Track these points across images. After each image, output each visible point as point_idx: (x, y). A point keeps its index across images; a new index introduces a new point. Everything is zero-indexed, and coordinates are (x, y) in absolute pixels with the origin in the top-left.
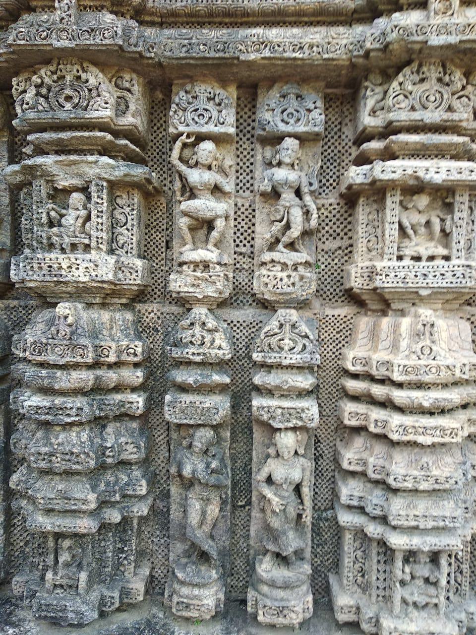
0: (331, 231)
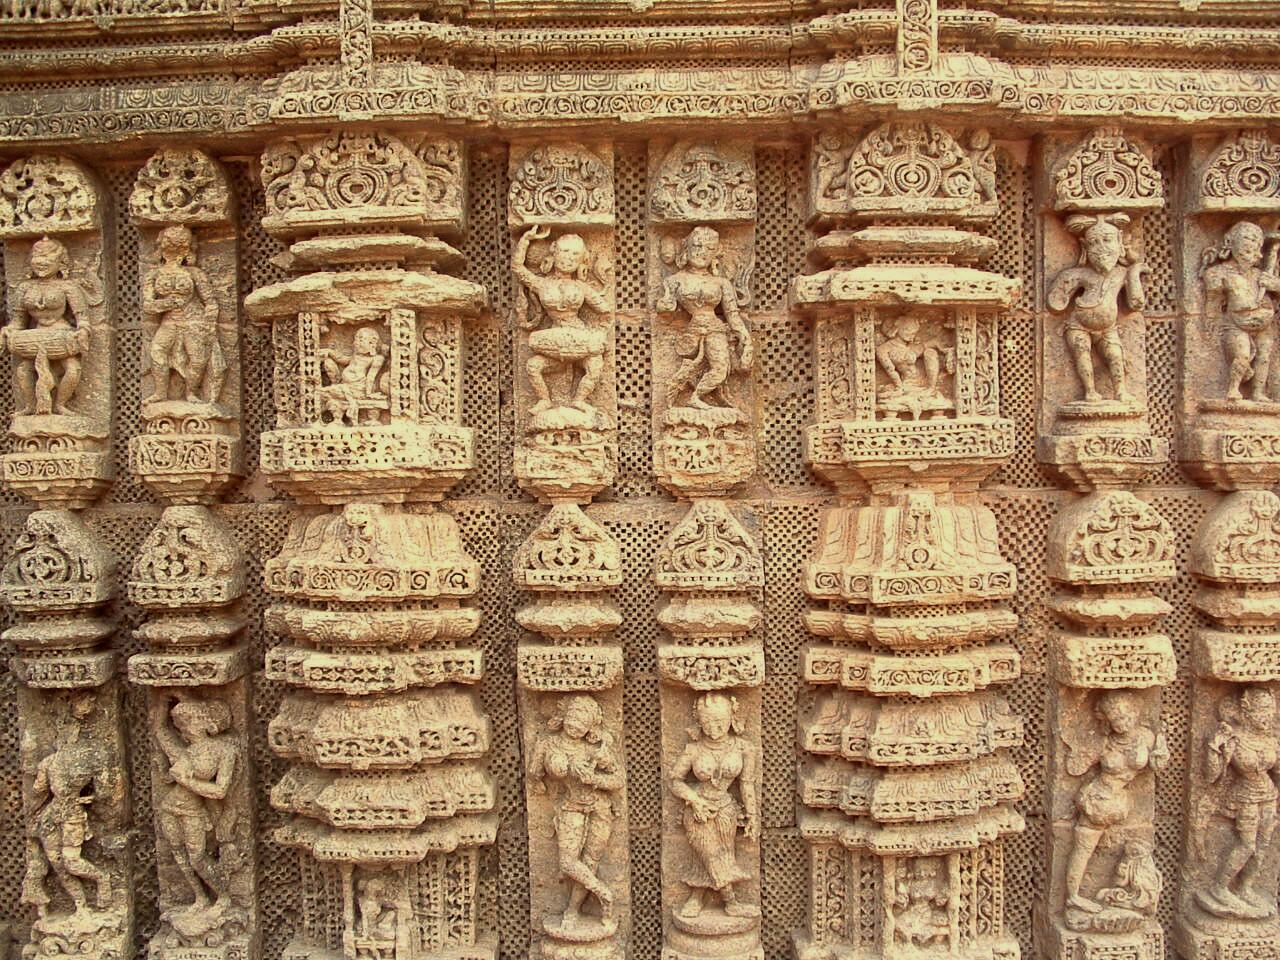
0: (778, 369)
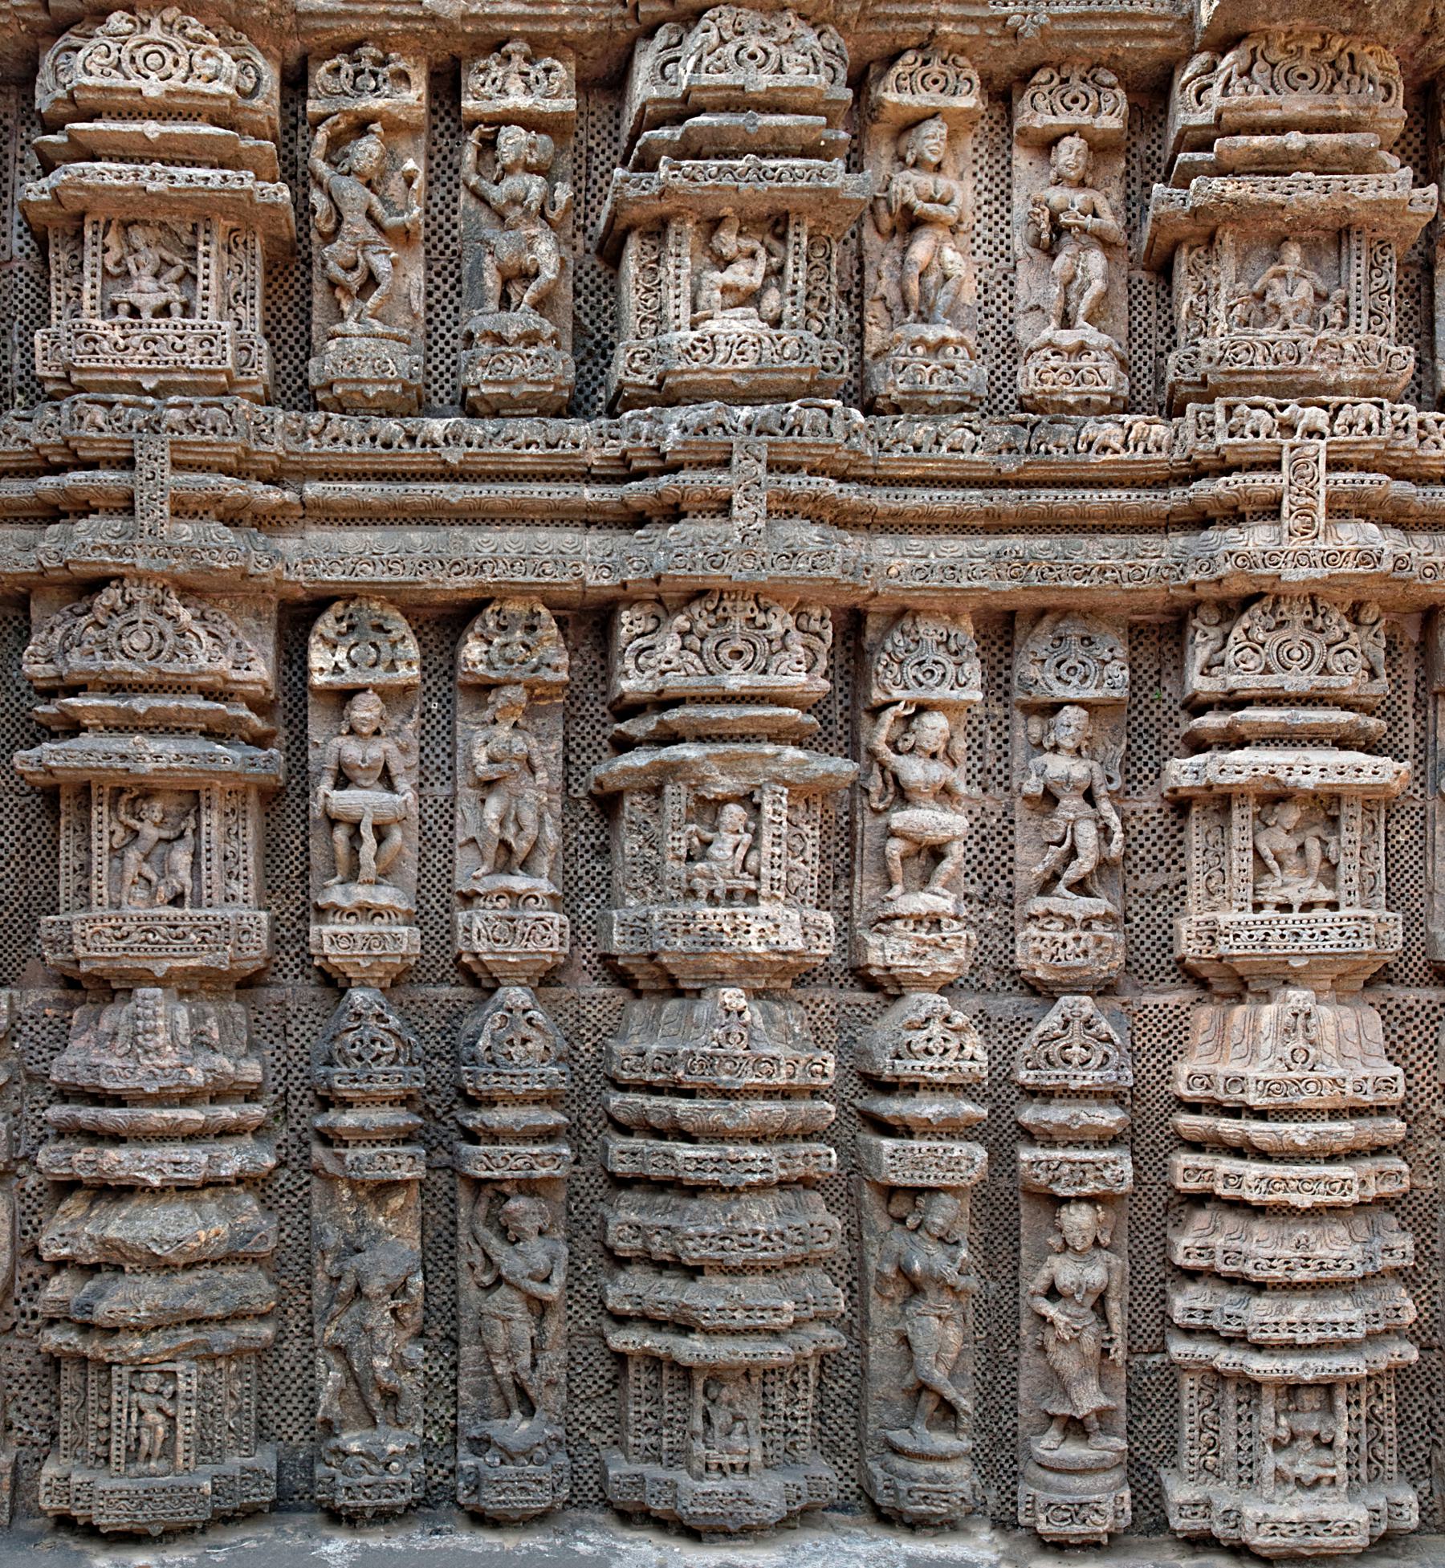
0: (1149, 858)
